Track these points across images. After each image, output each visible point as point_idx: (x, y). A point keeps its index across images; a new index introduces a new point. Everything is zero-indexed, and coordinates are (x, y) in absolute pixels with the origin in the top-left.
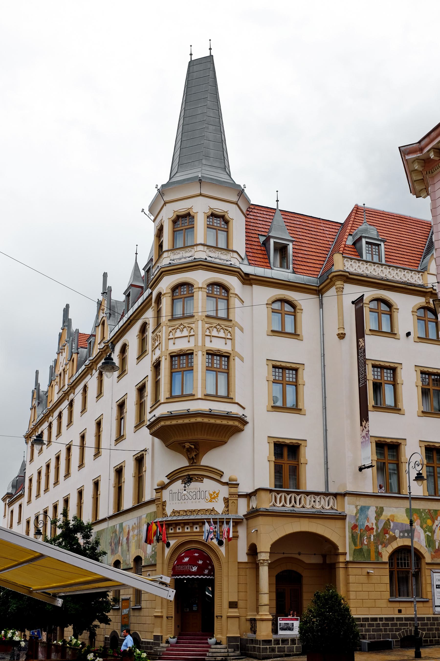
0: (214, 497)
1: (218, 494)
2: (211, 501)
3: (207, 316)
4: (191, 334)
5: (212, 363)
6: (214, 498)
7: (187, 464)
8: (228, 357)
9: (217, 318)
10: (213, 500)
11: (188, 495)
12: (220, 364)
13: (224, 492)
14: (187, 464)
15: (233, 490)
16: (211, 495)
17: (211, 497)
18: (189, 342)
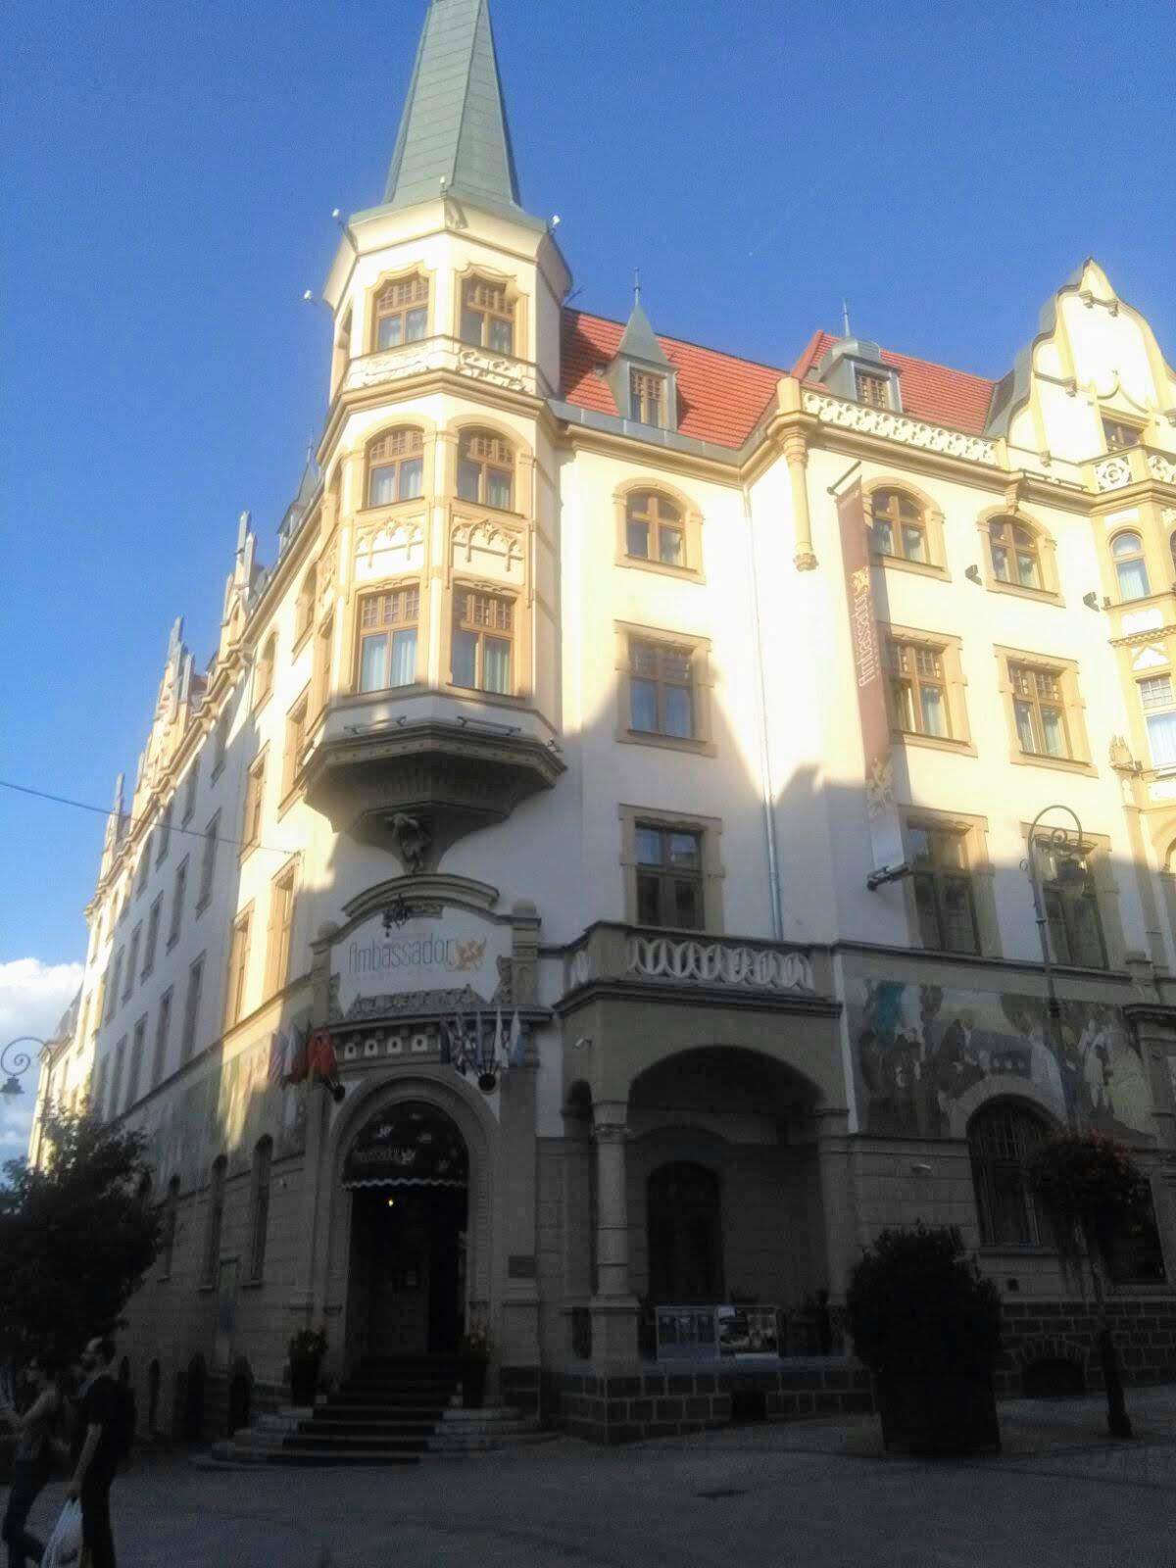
0: (470, 956)
1: (480, 949)
2: (461, 968)
4: (414, 540)
6: (470, 959)
10: (468, 964)
15: (528, 936)
16: (462, 951)
17: (462, 956)
18: (409, 558)
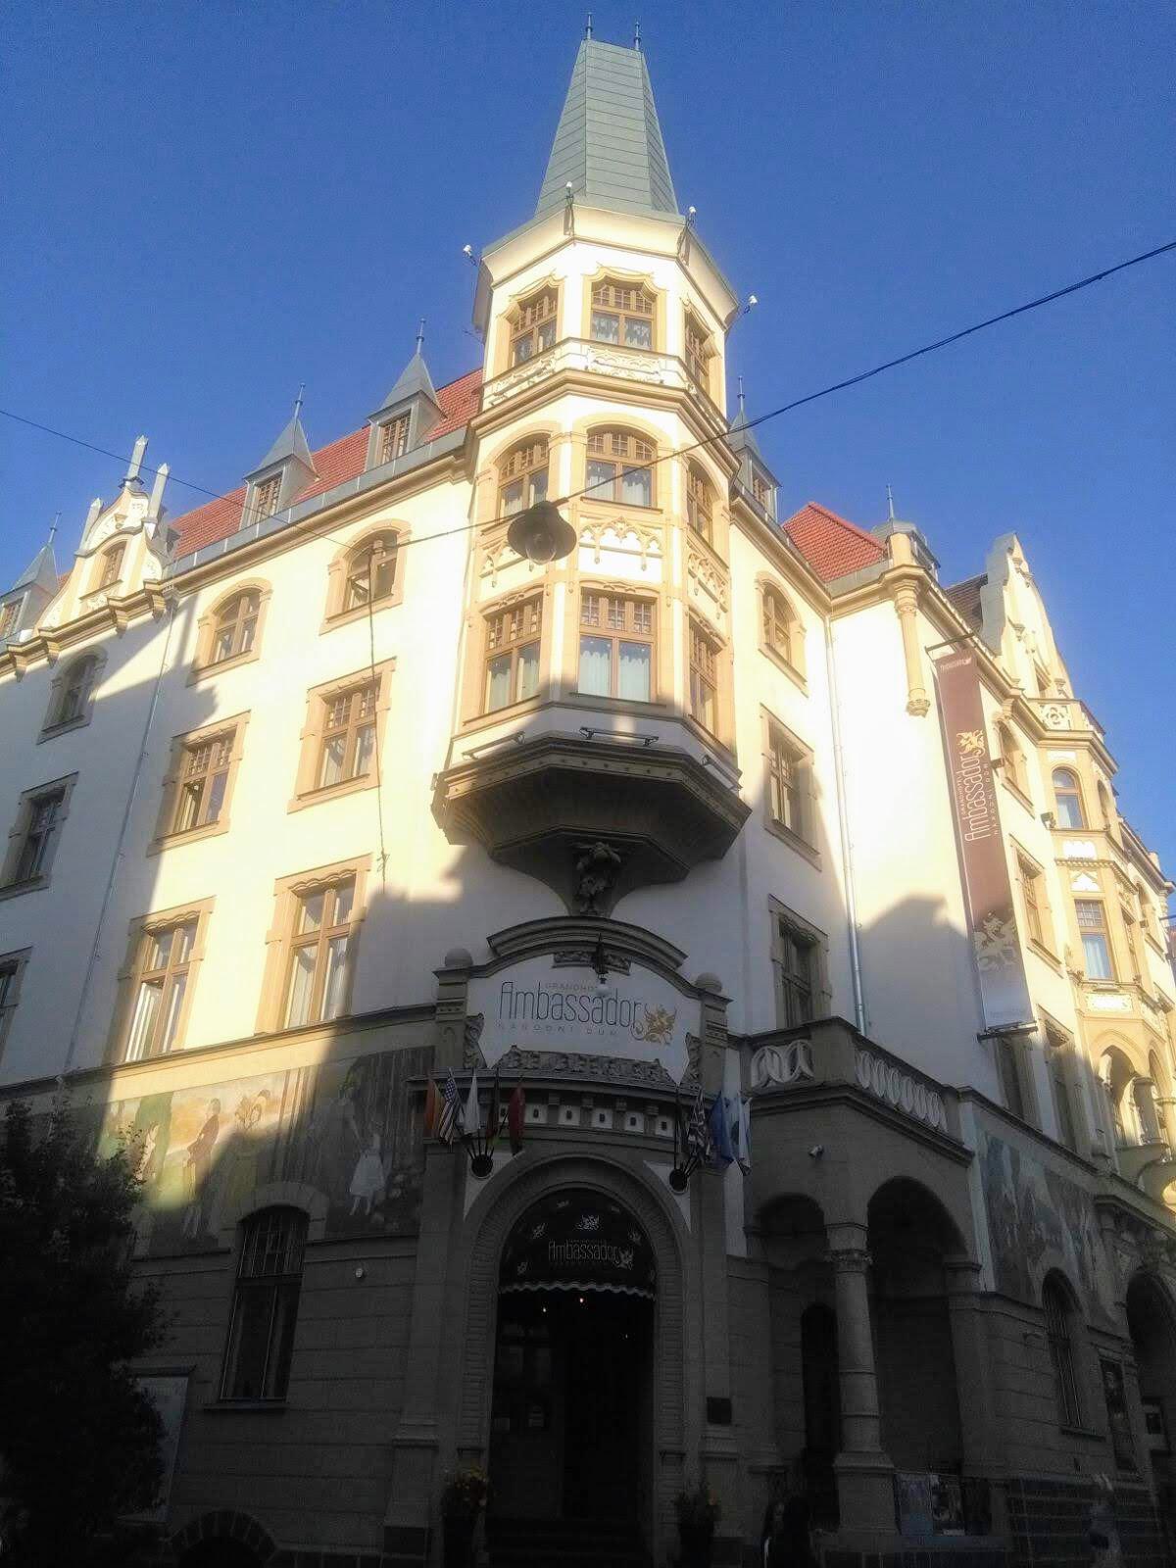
0: (659, 1026)
1: (671, 1020)
2: (650, 1038)
6: (660, 1030)
7: (563, 912)
11: (576, 1006)
13: (689, 1016)
16: (651, 1019)
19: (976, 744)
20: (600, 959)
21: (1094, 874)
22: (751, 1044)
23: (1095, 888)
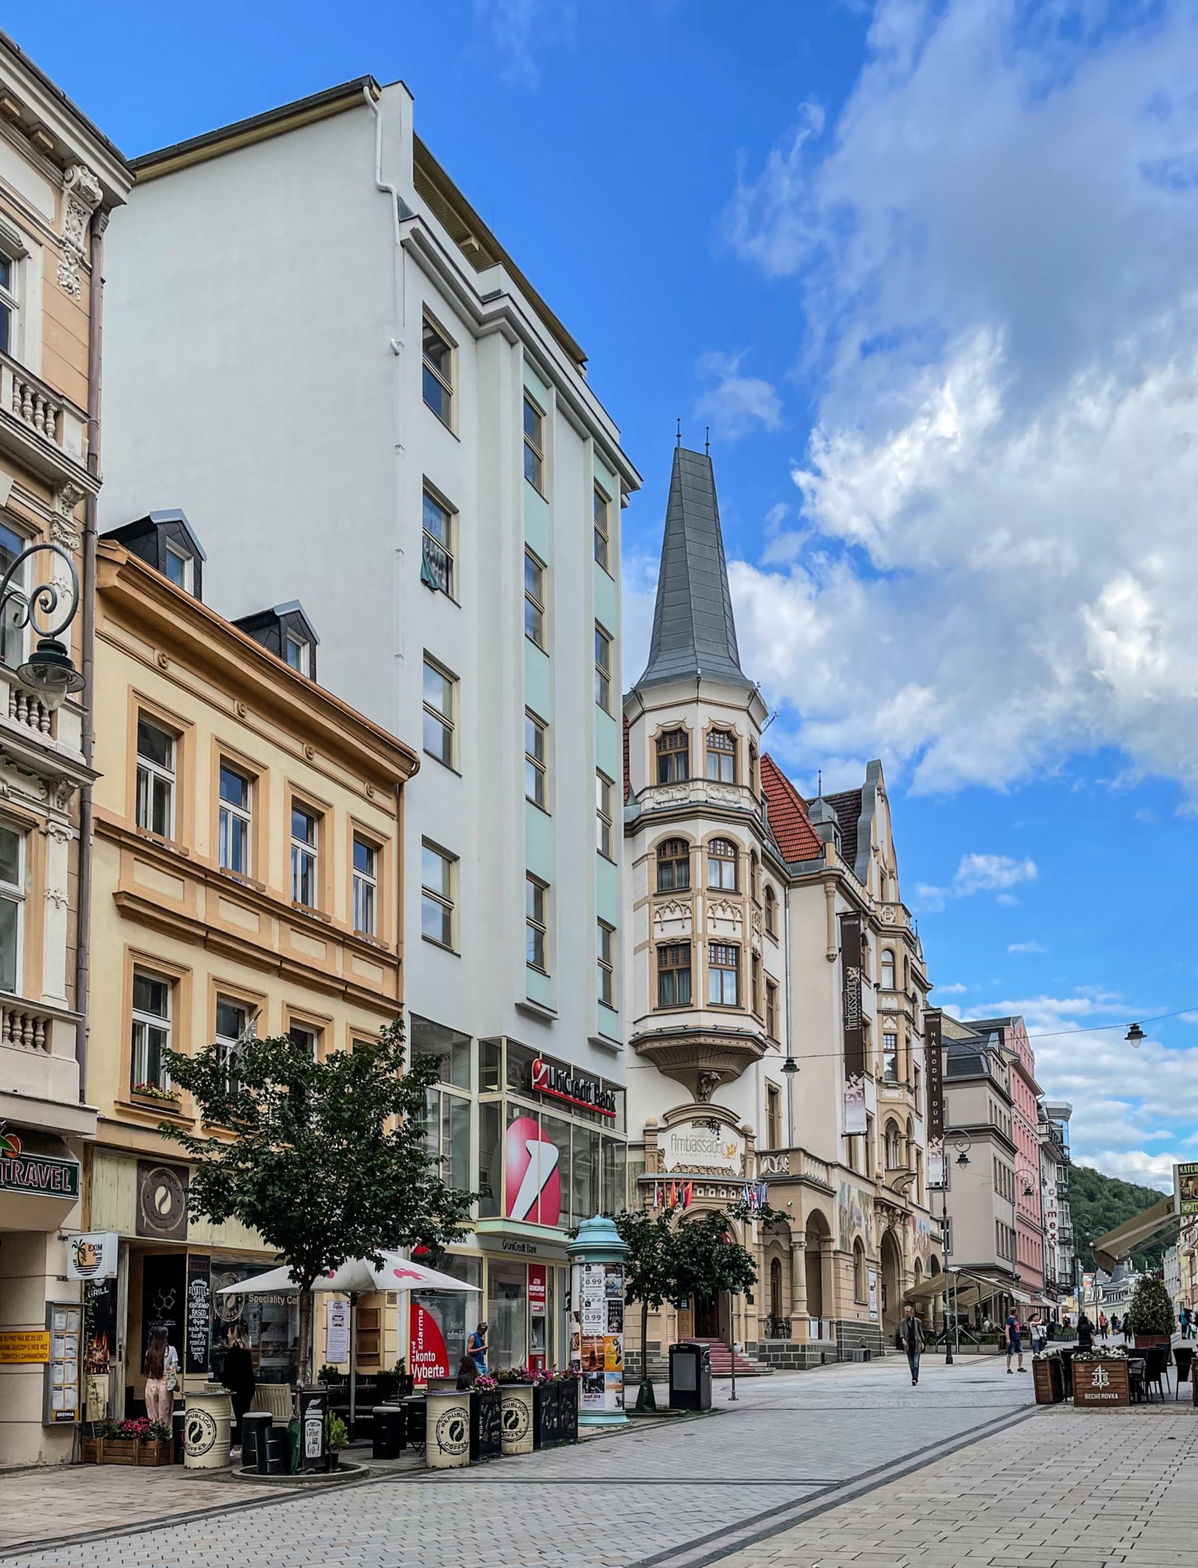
2: (728, 1157)
3: (710, 889)
5: (716, 958)
6: (732, 1153)
8: (737, 948)
9: (720, 890)
12: (727, 958)
14: (693, 1102)
16: (729, 1149)
19: (855, 975)
20: (712, 1124)
21: (894, 1018)
22: (760, 1154)
23: (894, 1026)
